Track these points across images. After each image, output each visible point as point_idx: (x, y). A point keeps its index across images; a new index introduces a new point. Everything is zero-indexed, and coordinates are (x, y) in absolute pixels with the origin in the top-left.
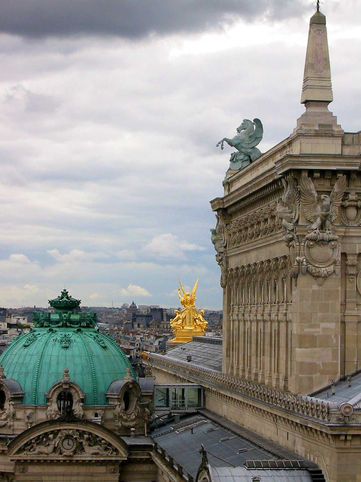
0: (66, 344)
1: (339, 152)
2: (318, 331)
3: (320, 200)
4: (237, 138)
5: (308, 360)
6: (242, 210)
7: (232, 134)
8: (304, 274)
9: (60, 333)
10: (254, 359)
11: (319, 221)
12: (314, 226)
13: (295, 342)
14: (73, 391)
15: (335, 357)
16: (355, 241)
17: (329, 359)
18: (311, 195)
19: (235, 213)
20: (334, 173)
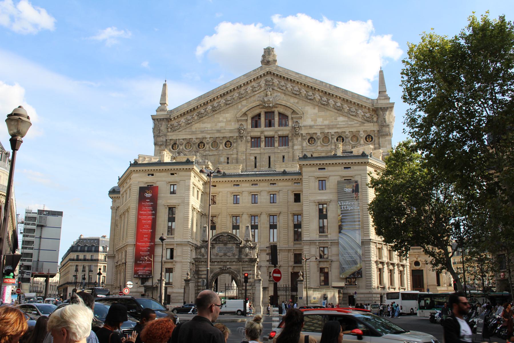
20: (163, 119)
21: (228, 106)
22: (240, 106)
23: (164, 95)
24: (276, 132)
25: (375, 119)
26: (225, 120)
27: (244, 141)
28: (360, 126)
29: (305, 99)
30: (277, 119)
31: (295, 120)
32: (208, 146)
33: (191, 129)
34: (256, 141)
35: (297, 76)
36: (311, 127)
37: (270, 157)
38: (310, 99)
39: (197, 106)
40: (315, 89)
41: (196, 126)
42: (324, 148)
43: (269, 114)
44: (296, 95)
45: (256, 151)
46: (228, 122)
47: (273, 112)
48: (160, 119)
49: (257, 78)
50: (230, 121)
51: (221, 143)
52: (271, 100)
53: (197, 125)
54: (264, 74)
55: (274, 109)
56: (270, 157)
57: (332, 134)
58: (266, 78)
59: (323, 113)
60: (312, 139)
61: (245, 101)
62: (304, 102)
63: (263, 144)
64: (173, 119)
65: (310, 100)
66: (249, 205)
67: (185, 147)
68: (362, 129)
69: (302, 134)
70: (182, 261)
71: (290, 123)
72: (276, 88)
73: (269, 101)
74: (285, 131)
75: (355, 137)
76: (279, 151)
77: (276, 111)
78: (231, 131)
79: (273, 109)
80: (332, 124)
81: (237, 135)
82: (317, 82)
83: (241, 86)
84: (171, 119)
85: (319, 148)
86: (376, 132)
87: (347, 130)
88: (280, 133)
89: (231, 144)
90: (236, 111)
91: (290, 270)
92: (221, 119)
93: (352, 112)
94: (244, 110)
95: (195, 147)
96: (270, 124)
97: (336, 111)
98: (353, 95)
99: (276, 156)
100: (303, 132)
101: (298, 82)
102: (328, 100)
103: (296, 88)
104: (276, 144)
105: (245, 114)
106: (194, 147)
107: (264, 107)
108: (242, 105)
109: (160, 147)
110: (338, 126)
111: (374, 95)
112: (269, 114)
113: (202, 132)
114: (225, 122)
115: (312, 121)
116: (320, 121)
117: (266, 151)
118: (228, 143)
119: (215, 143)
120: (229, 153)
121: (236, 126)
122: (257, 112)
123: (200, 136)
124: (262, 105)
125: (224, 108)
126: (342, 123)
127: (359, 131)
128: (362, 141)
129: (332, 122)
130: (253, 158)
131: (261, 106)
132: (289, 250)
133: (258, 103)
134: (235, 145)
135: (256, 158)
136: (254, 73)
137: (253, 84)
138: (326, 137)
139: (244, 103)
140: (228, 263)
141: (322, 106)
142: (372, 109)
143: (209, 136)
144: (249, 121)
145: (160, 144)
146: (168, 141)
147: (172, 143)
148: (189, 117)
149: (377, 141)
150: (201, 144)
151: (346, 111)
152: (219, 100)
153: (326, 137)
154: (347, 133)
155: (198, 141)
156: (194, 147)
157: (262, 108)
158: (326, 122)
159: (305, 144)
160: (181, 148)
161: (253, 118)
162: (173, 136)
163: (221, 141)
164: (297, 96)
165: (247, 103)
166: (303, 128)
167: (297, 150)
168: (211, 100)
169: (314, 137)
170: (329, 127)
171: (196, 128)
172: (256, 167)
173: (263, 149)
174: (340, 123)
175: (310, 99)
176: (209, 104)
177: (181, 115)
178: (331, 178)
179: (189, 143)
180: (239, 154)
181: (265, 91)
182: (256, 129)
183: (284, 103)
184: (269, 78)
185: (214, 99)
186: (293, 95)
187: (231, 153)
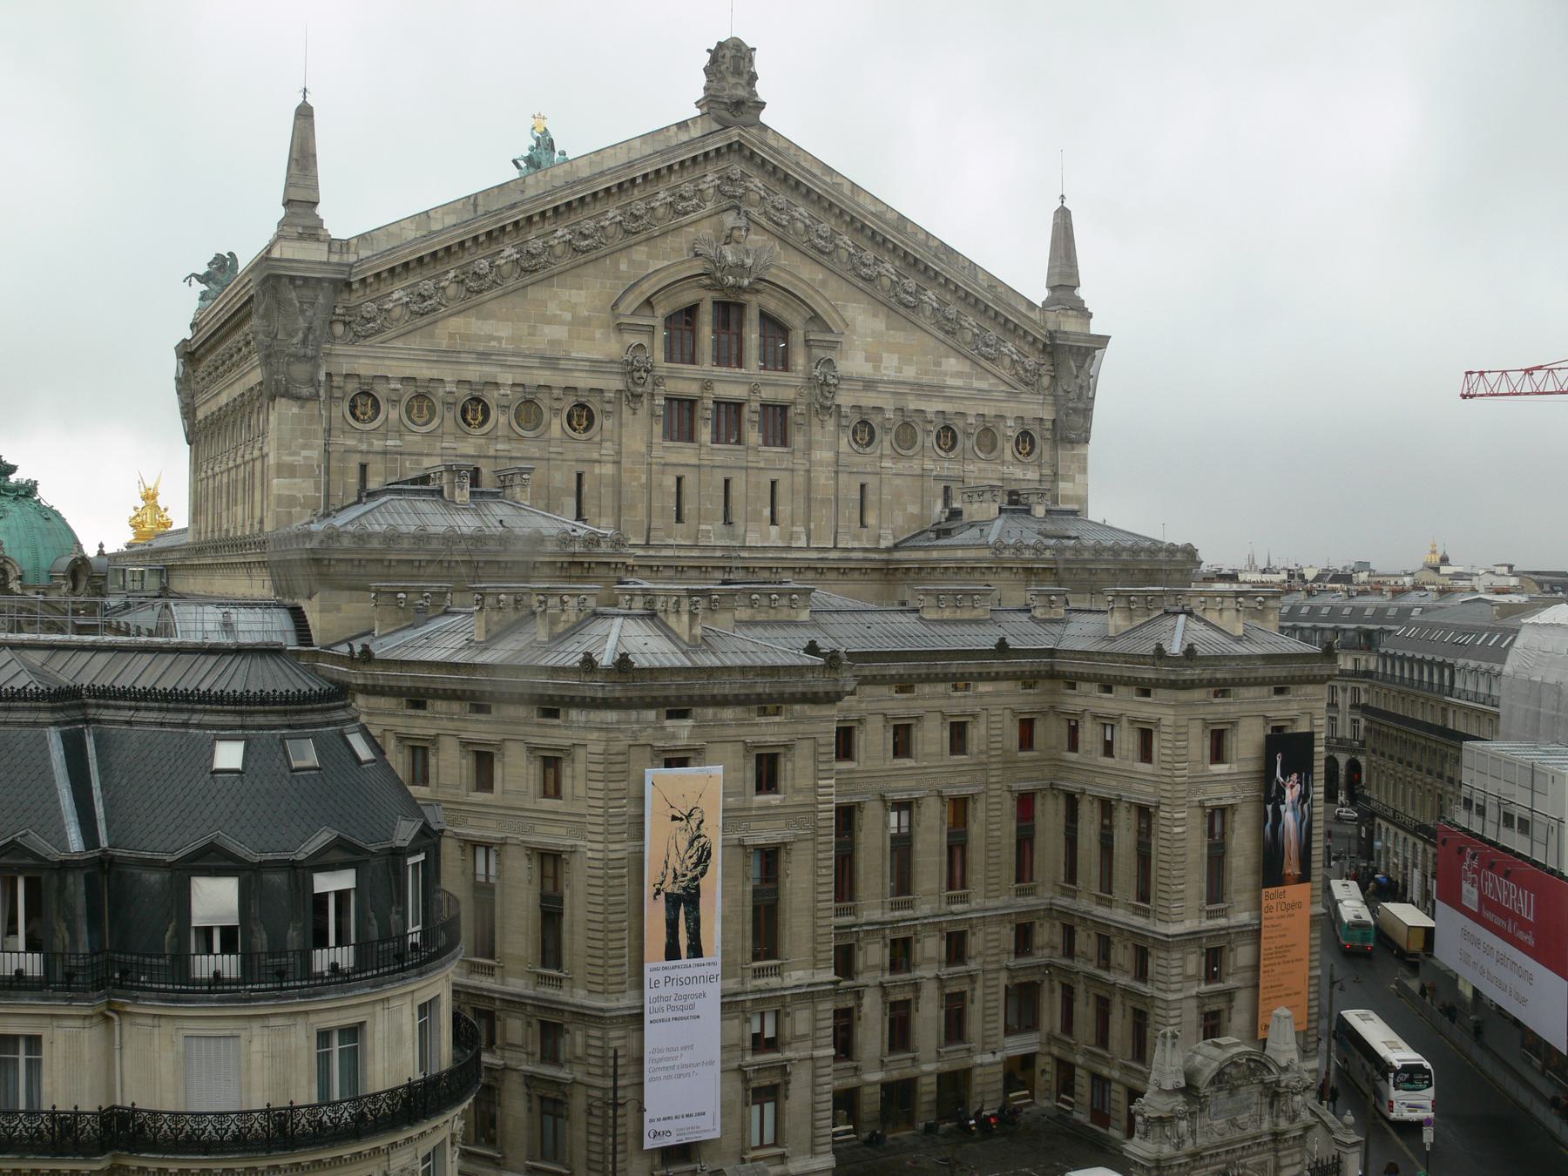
1: (324, 259)
2: (298, 460)
3: (302, 312)
4: (208, 274)
5: (287, 492)
6: (214, 348)
7: (202, 269)
8: (282, 396)
10: (224, 514)
11: (301, 335)
12: (295, 341)
13: (272, 472)
14: (8, 567)
15: (317, 489)
16: (341, 360)
17: (311, 493)
18: (292, 305)
19: (204, 355)
20: (319, 280)
21: (581, 258)
22: (623, 267)
23: (303, 159)
24: (754, 389)
25: (1046, 381)
26: (568, 316)
27: (643, 411)
28: (1013, 396)
29: (850, 276)
30: (752, 336)
31: (819, 353)
32: (503, 419)
33: (432, 336)
34: (681, 417)
35: (828, 179)
36: (869, 385)
37: (727, 482)
38: (868, 279)
39: (462, 244)
40: (885, 240)
41: (455, 327)
42: (900, 465)
43: (729, 312)
44: (820, 254)
45: (684, 454)
46: (579, 324)
47: (741, 307)
48: (305, 279)
49: (694, 158)
50: (587, 322)
51: (557, 412)
52: (749, 262)
53: (455, 323)
54: (718, 150)
55: (746, 297)
56: (727, 482)
57: (929, 416)
58: (723, 164)
59: (898, 337)
60: (864, 430)
61: (643, 248)
62: (845, 285)
63: (705, 433)
64: (355, 286)
66: (888, 765)
67: (409, 411)
68: (1011, 409)
69: (839, 406)
70: (817, 1053)
71: (799, 360)
72: (755, 213)
73: (743, 266)
74: (785, 387)
75: (988, 436)
76: (762, 465)
77: (753, 304)
78: (596, 366)
79: (746, 297)
80: (925, 379)
81: (621, 386)
82: (889, 215)
83: (633, 180)
84: (348, 285)
85: (887, 463)
86: (1049, 425)
87: (972, 409)
88: (767, 394)
89: (591, 418)
90: (608, 283)
91: (1003, 979)
92: (553, 308)
93: (988, 346)
94: (647, 288)
95: (451, 418)
96: (731, 355)
97: (941, 335)
98: (994, 283)
99: (752, 479)
100: (844, 399)
101: (831, 205)
102: (921, 289)
103: (825, 228)
104: (753, 436)
105: (648, 302)
106: (449, 416)
107: (717, 285)
108: (632, 262)
109: (302, 407)
110: (948, 393)
111: (1038, 293)
112: (729, 312)
113: (484, 357)
114: (568, 327)
115: (867, 360)
116: (890, 367)
117: (719, 459)
118: (582, 415)
119: (528, 410)
120: (586, 456)
121: (610, 347)
122: (687, 298)
123: (474, 372)
124: (710, 278)
125: (566, 262)
126: (959, 382)
127: (1002, 417)
128: (1009, 450)
129: (926, 372)
130: (670, 482)
131: (708, 282)
132: (1002, 919)
133: (697, 267)
134: (608, 424)
135: (679, 480)
136: (684, 137)
137: (674, 179)
138: (906, 424)
139: (640, 253)
140: (1239, 1153)
141: (902, 310)
142: (1045, 345)
143: (507, 378)
144: (661, 334)
145: (306, 391)
146: (337, 381)
147: (352, 387)
148: (427, 286)
149: (1046, 457)
150: (474, 409)
151: (969, 337)
152: (548, 228)
153: (906, 424)
154: (971, 420)
155: (463, 394)
156: (449, 416)
157: (705, 287)
158: (910, 373)
159: (844, 442)
160: (394, 415)
161: (669, 320)
163: (556, 405)
164: (824, 259)
165: (650, 256)
166: (843, 385)
167: (821, 463)
168: (516, 223)
169: (875, 420)
170: (921, 390)
171: (452, 336)
172: (679, 519)
173: (704, 454)
174: (950, 382)
175: (868, 279)
176: (507, 241)
177: (392, 270)
178: (1244, 723)
179: (421, 400)
180: (626, 463)
181: (714, 219)
182: (687, 369)
183: (783, 280)
184: (737, 168)
185: (529, 219)
186: (812, 253)
187: (595, 456)
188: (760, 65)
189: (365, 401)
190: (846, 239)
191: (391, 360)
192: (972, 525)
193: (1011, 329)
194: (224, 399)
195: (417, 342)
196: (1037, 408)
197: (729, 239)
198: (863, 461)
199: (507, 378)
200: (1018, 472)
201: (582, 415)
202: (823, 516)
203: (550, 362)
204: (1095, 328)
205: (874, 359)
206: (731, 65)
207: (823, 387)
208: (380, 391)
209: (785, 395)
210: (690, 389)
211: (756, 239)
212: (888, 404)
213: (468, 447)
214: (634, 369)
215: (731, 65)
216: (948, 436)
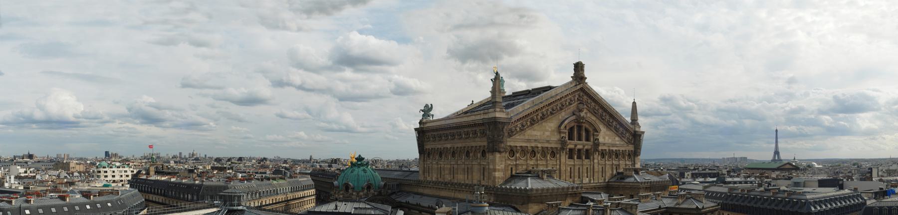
0: (364, 171)
9: (362, 168)
44: (594, 113)
45: (571, 162)
59: (608, 133)
60: (603, 154)
65: (601, 118)
74: (588, 145)
87: (621, 149)
100: (600, 148)
106: (529, 155)
111: (629, 119)
112: (580, 128)
118: (553, 154)
122: (572, 125)
123: (533, 145)
139: (563, 114)
150: (533, 153)
158: (610, 141)
162: (511, 142)
170: (614, 145)
188: (586, 69)
189: (512, 152)
190: (600, 111)
191: (517, 141)
192: (629, 177)
193: (627, 130)
194: (449, 146)
195: (522, 137)
196: (631, 148)
197: (581, 111)
198: (602, 162)
199: (539, 145)
200: (627, 163)
201: (553, 154)
202: (596, 174)
203: (548, 142)
204: (642, 129)
205: (604, 138)
206: (579, 67)
207: (596, 144)
208: (515, 149)
209: (589, 147)
210: (572, 146)
211: (585, 111)
212: (607, 148)
213: (531, 163)
214: (563, 143)
215: (579, 67)
216: (617, 156)
